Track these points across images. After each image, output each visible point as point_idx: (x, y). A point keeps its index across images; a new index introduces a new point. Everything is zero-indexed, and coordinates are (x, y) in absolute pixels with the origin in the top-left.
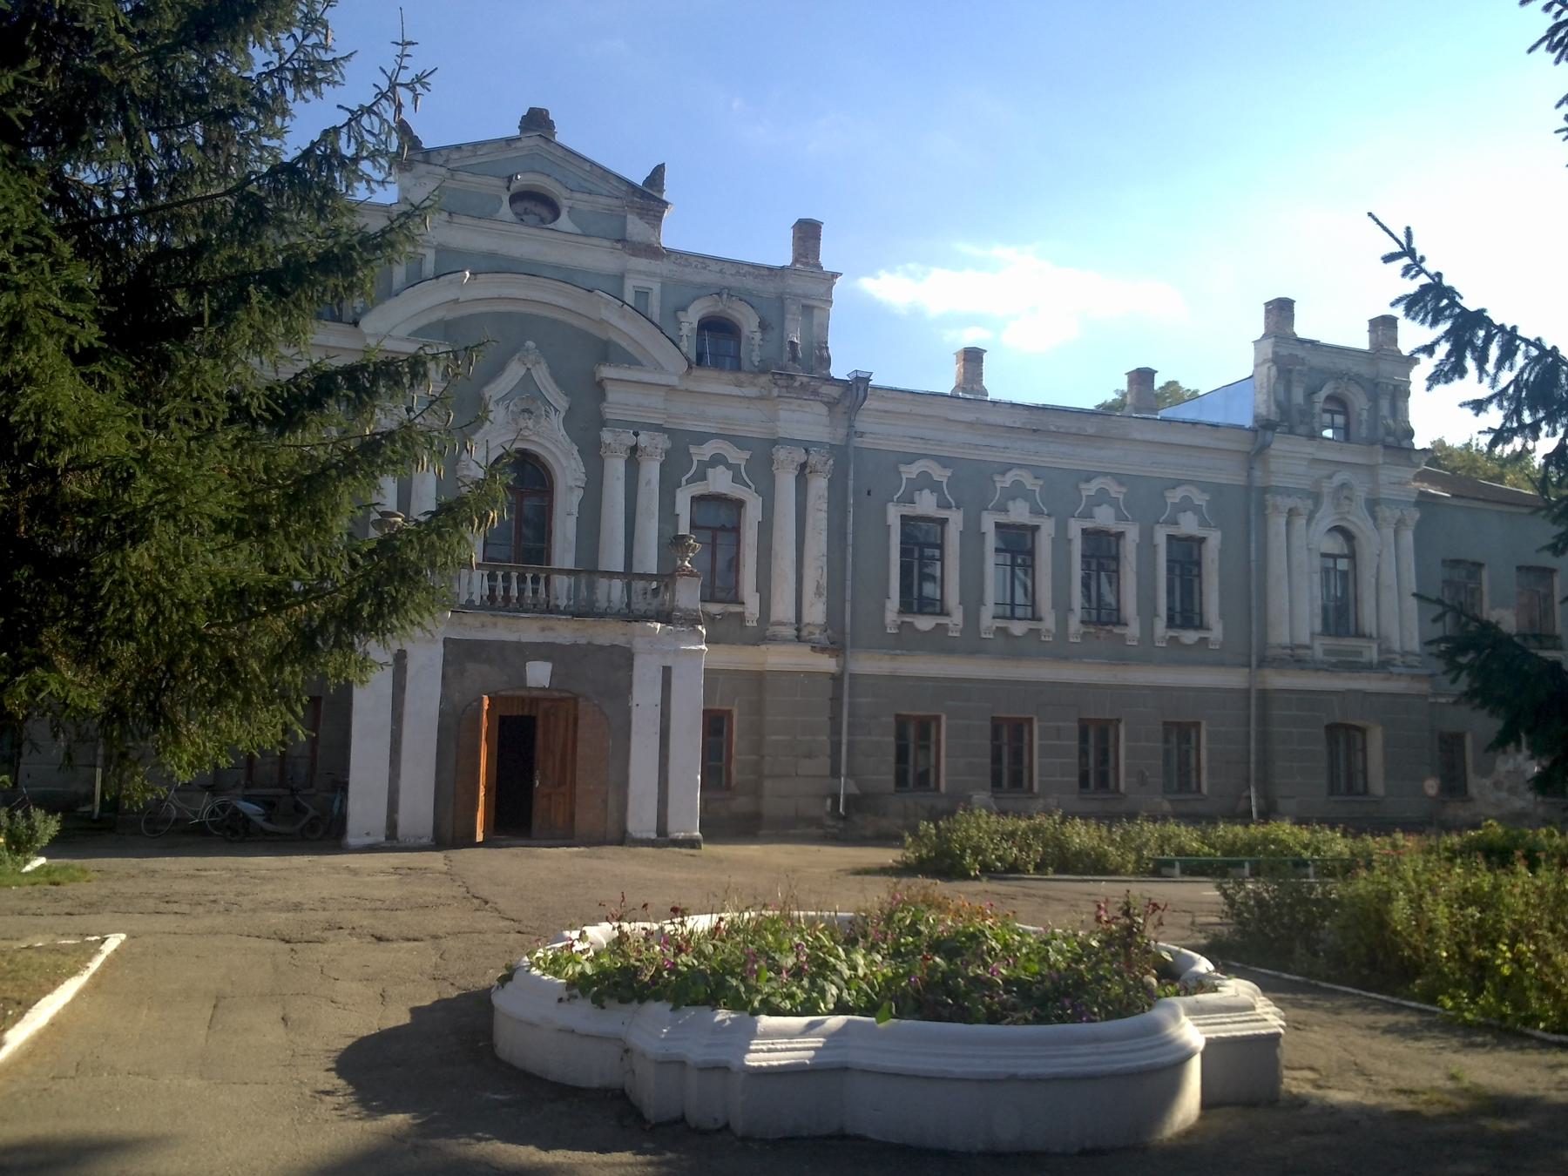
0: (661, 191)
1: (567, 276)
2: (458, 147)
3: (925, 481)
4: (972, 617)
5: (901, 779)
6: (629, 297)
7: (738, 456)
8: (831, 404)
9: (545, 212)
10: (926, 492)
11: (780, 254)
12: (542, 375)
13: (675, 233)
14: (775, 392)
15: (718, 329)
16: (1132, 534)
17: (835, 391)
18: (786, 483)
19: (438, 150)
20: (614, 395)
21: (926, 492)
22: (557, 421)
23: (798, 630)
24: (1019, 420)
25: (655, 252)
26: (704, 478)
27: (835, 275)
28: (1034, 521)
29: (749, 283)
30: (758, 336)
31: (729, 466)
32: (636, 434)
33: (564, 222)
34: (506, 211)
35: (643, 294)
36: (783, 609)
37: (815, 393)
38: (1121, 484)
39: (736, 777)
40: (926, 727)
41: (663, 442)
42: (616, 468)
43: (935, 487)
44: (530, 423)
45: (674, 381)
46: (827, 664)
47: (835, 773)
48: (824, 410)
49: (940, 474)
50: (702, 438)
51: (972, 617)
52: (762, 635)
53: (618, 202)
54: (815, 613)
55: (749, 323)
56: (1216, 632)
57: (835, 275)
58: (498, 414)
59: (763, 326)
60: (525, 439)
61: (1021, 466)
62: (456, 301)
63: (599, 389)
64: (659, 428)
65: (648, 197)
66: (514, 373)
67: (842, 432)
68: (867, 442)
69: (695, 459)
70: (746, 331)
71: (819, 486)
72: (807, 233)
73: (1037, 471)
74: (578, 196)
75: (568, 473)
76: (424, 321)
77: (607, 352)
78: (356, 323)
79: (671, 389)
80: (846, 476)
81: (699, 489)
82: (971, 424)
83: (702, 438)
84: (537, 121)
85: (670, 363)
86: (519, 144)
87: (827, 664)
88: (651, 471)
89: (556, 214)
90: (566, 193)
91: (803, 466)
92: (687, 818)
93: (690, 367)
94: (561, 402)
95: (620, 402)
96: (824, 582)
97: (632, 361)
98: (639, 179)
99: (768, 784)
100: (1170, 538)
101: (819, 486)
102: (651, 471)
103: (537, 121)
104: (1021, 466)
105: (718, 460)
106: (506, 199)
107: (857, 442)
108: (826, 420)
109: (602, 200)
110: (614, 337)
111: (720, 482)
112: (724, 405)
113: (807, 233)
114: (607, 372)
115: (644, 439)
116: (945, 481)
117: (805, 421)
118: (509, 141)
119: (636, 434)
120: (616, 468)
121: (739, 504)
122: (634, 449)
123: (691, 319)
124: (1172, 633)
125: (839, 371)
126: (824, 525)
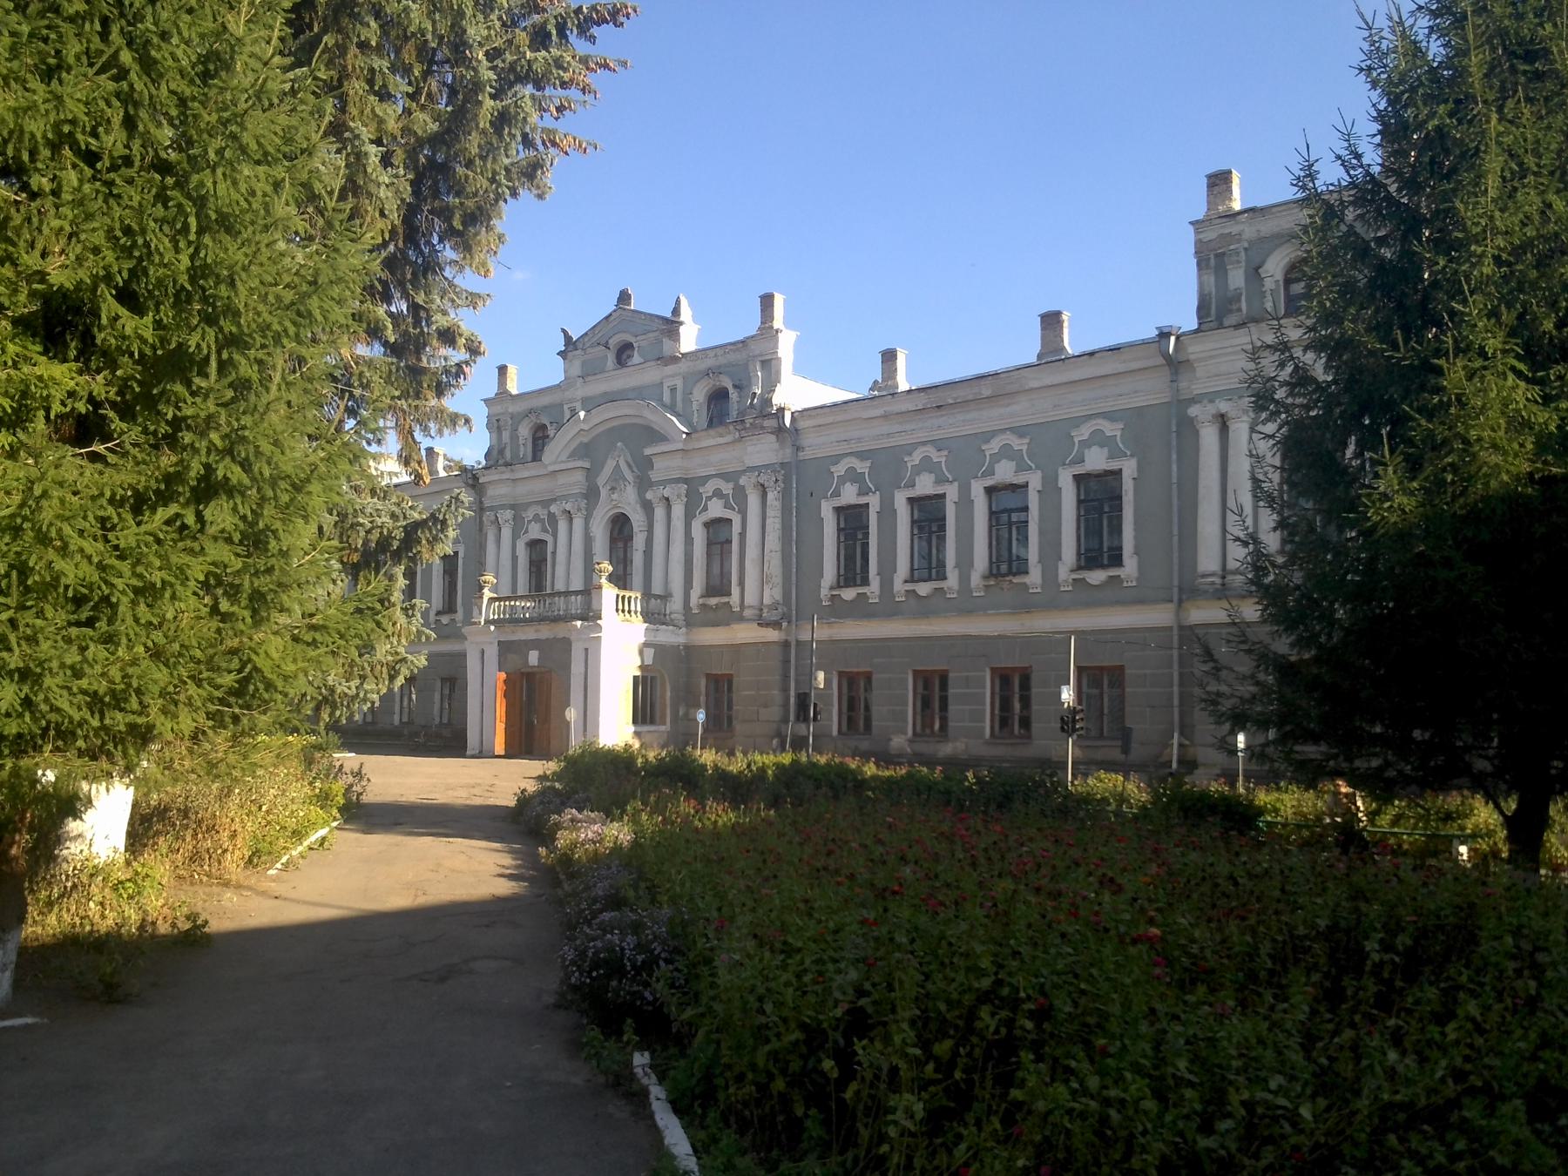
3: (1098, 439)
16: (952, 493)
20: (659, 464)
24: (921, 401)
28: (1114, 465)
37: (763, 428)
38: (1021, 436)
45: (680, 446)
48: (773, 438)
50: (705, 479)
60: (616, 507)
61: (924, 443)
63: (648, 463)
73: (938, 444)
75: (637, 519)
82: (885, 416)
83: (705, 479)
95: (658, 472)
100: (911, 500)
104: (924, 443)
108: (776, 446)
112: (722, 453)
116: (1119, 433)
117: (763, 451)
124: (910, 587)
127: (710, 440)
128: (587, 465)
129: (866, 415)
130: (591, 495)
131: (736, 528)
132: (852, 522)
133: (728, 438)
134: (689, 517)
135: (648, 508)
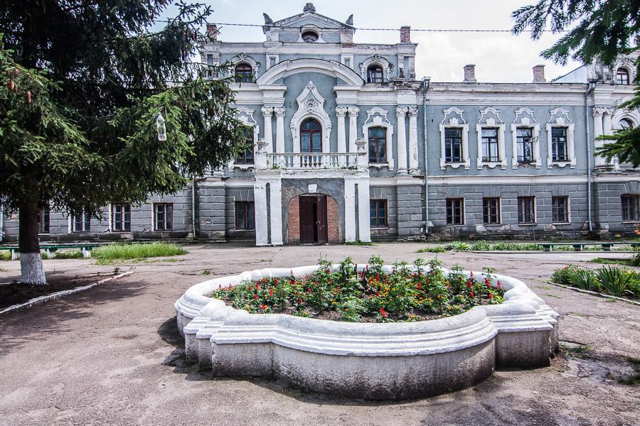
0: (352, 24)
1: (321, 58)
2: (284, 20)
4: (474, 162)
5: (449, 220)
6: (343, 62)
7: (383, 112)
8: (417, 91)
9: (314, 38)
10: (454, 119)
11: (396, 38)
12: (315, 91)
13: (356, 38)
14: (396, 88)
15: (373, 68)
17: (418, 86)
18: (401, 120)
19: (277, 22)
20: (340, 96)
21: (454, 119)
22: (321, 106)
23: (409, 170)
25: (351, 45)
26: (372, 121)
27: (416, 45)
29: (385, 52)
30: (389, 70)
31: (380, 116)
32: (347, 108)
33: (320, 40)
34: (301, 40)
35: (347, 60)
36: (402, 164)
39: (389, 222)
40: (458, 202)
41: (357, 110)
42: (341, 120)
43: (458, 116)
44: (312, 108)
45: (359, 88)
46: (421, 182)
47: (424, 219)
48: (414, 93)
49: (459, 111)
50: (370, 107)
51: (474, 162)
52: (396, 174)
53: (337, 30)
54: (414, 164)
55: (385, 66)
56: (573, 162)
57: (416, 45)
58: (301, 106)
59: (391, 66)
60: (311, 114)
61: (491, 106)
62: (286, 71)
63: (335, 93)
64: (355, 105)
65: (348, 27)
66: (306, 91)
67: (421, 99)
68: (431, 103)
69: (369, 115)
70: (384, 68)
71: (413, 120)
72: (405, 31)
74: (323, 30)
75: (326, 123)
76: (276, 79)
77: (336, 81)
78: (255, 82)
79: (359, 91)
80: (424, 115)
81: (371, 125)
83: (370, 107)
84: (309, 8)
85: (357, 83)
86: (303, 16)
87: (421, 182)
88: (353, 120)
89: (317, 36)
90: (320, 30)
91: (407, 113)
92: (365, 235)
93: (364, 83)
94: (322, 100)
95: (341, 98)
96: (417, 153)
97: (344, 83)
98: (344, 22)
99: (399, 223)
101: (413, 120)
102: (353, 120)
103: (309, 8)
104: (491, 106)
105: (377, 114)
106: (300, 35)
107: (427, 103)
109: (331, 30)
110: (338, 76)
111: (378, 122)
113: (405, 31)
114: (336, 88)
115: (350, 110)
117: (408, 98)
118: (300, 15)
119: (347, 108)
120: (341, 120)
121: (385, 129)
122: (347, 113)
123: (365, 66)
125: (418, 78)
126: (416, 133)
127: (372, 88)
128: (285, 88)
129: (463, 90)
130: (291, 105)
131: (390, 132)
132: (454, 135)
133: (388, 89)
134: (360, 124)
135: (334, 117)
